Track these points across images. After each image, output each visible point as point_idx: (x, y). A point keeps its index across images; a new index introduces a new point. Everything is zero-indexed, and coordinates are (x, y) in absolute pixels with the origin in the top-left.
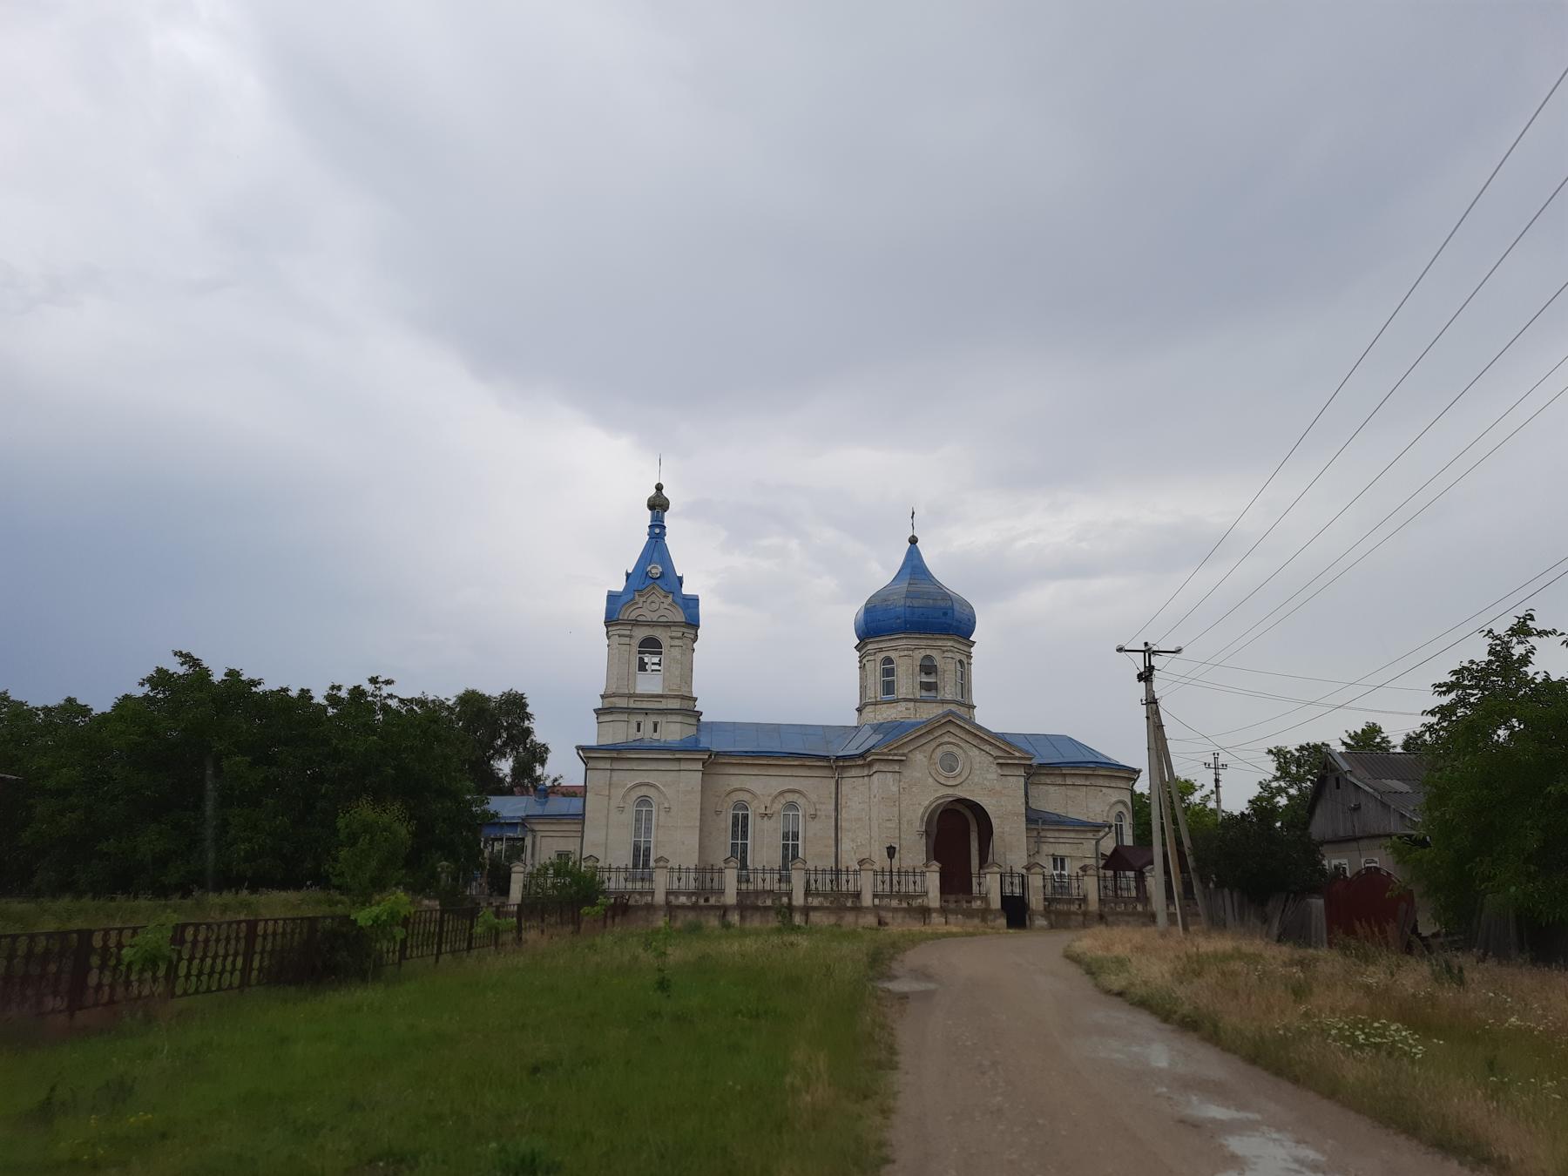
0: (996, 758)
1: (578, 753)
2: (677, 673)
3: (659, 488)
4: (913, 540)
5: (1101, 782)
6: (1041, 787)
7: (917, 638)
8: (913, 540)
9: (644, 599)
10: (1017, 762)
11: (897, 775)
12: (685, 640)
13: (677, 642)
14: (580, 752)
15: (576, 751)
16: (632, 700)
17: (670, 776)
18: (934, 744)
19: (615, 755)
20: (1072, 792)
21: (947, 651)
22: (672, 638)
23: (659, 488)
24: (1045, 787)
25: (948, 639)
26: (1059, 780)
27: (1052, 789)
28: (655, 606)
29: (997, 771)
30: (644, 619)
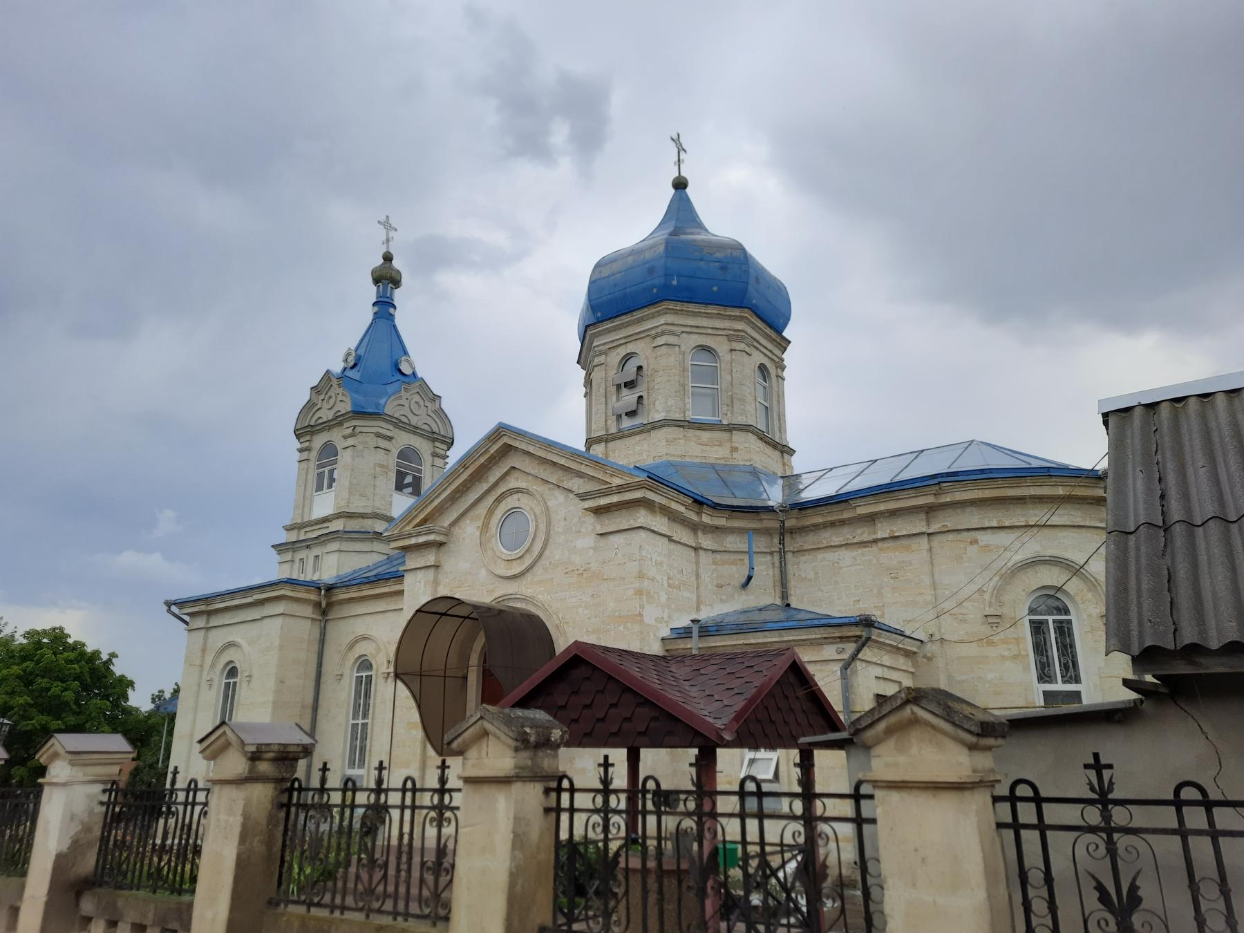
0: (583, 497)
1: (169, 611)
2: (347, 484)
3: (388, 258)
4: (680, 184)
5: (973, 518)
6: (820, 555)
7: (609, 331)
8: (680, 184)
9: (322, 397)
10: (615, 499)
11: (431, 572)
12: (361, 438)
13: (350, 442)
14: (174, 608)
15: (166, 608)
16: (303, 531)
17: (253, 629)
18: (490, 500)
19: (203, 608)
20: (890, 556)
21: (658, 335)
22: (345, 437)
23: (388, 258)
24: (831, 556)
25: (659, 314)
26: (863, 534)
27: (846, 556)
28: (332, 401)
29: (594, 529)
30: (321, 421)
